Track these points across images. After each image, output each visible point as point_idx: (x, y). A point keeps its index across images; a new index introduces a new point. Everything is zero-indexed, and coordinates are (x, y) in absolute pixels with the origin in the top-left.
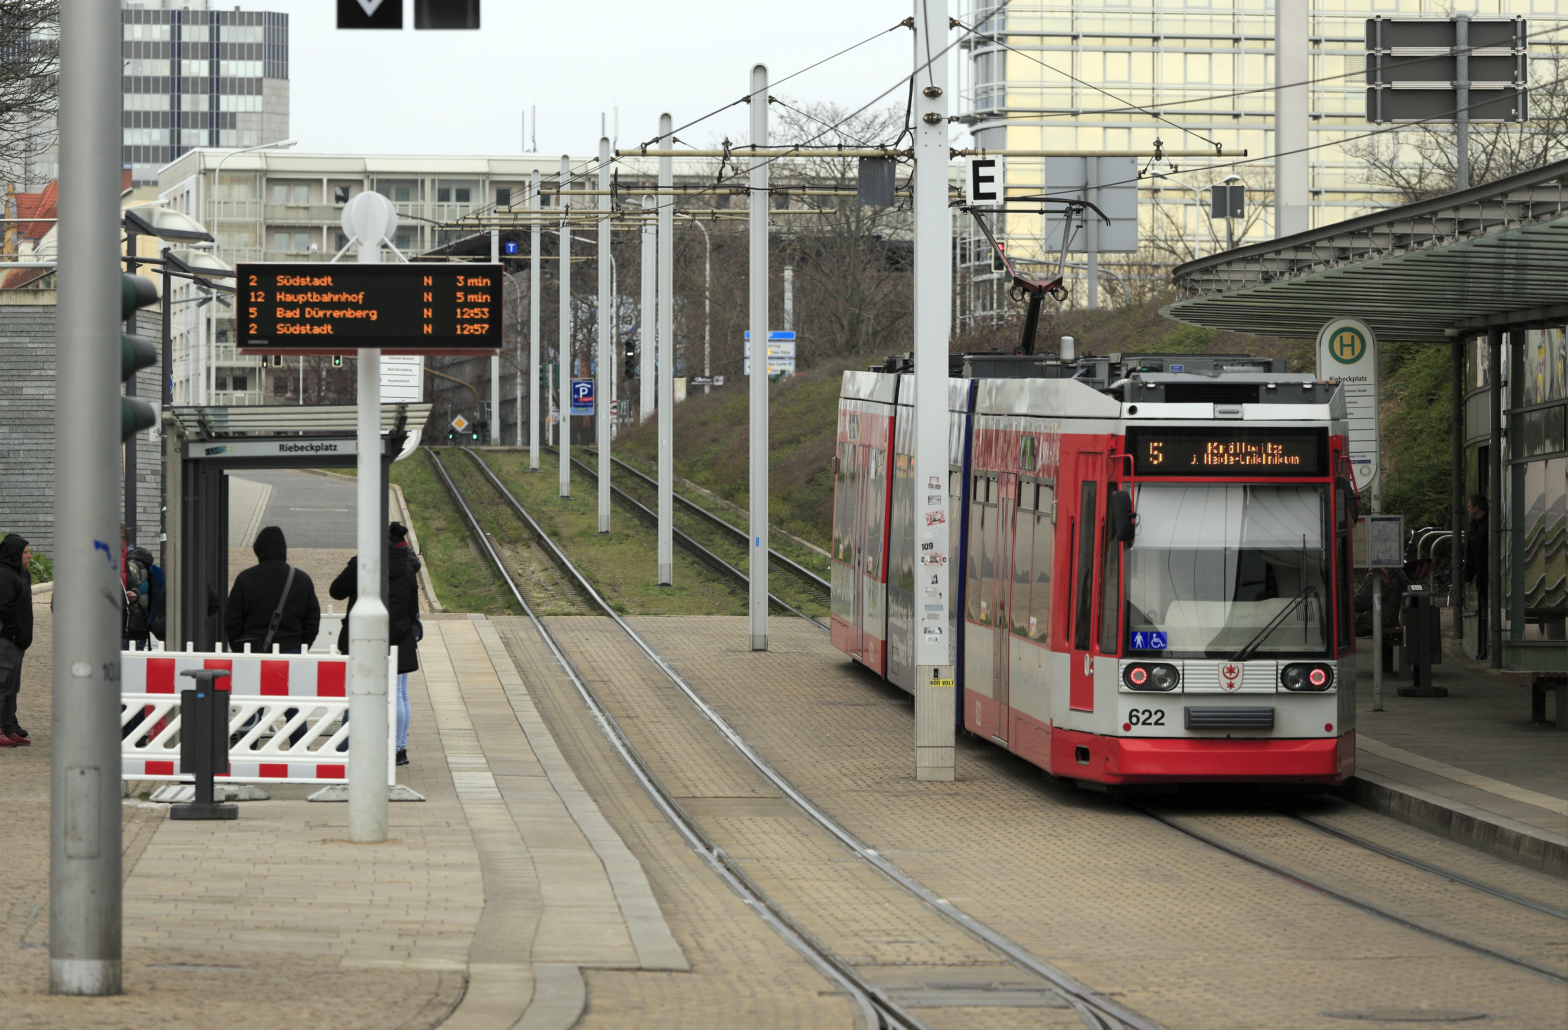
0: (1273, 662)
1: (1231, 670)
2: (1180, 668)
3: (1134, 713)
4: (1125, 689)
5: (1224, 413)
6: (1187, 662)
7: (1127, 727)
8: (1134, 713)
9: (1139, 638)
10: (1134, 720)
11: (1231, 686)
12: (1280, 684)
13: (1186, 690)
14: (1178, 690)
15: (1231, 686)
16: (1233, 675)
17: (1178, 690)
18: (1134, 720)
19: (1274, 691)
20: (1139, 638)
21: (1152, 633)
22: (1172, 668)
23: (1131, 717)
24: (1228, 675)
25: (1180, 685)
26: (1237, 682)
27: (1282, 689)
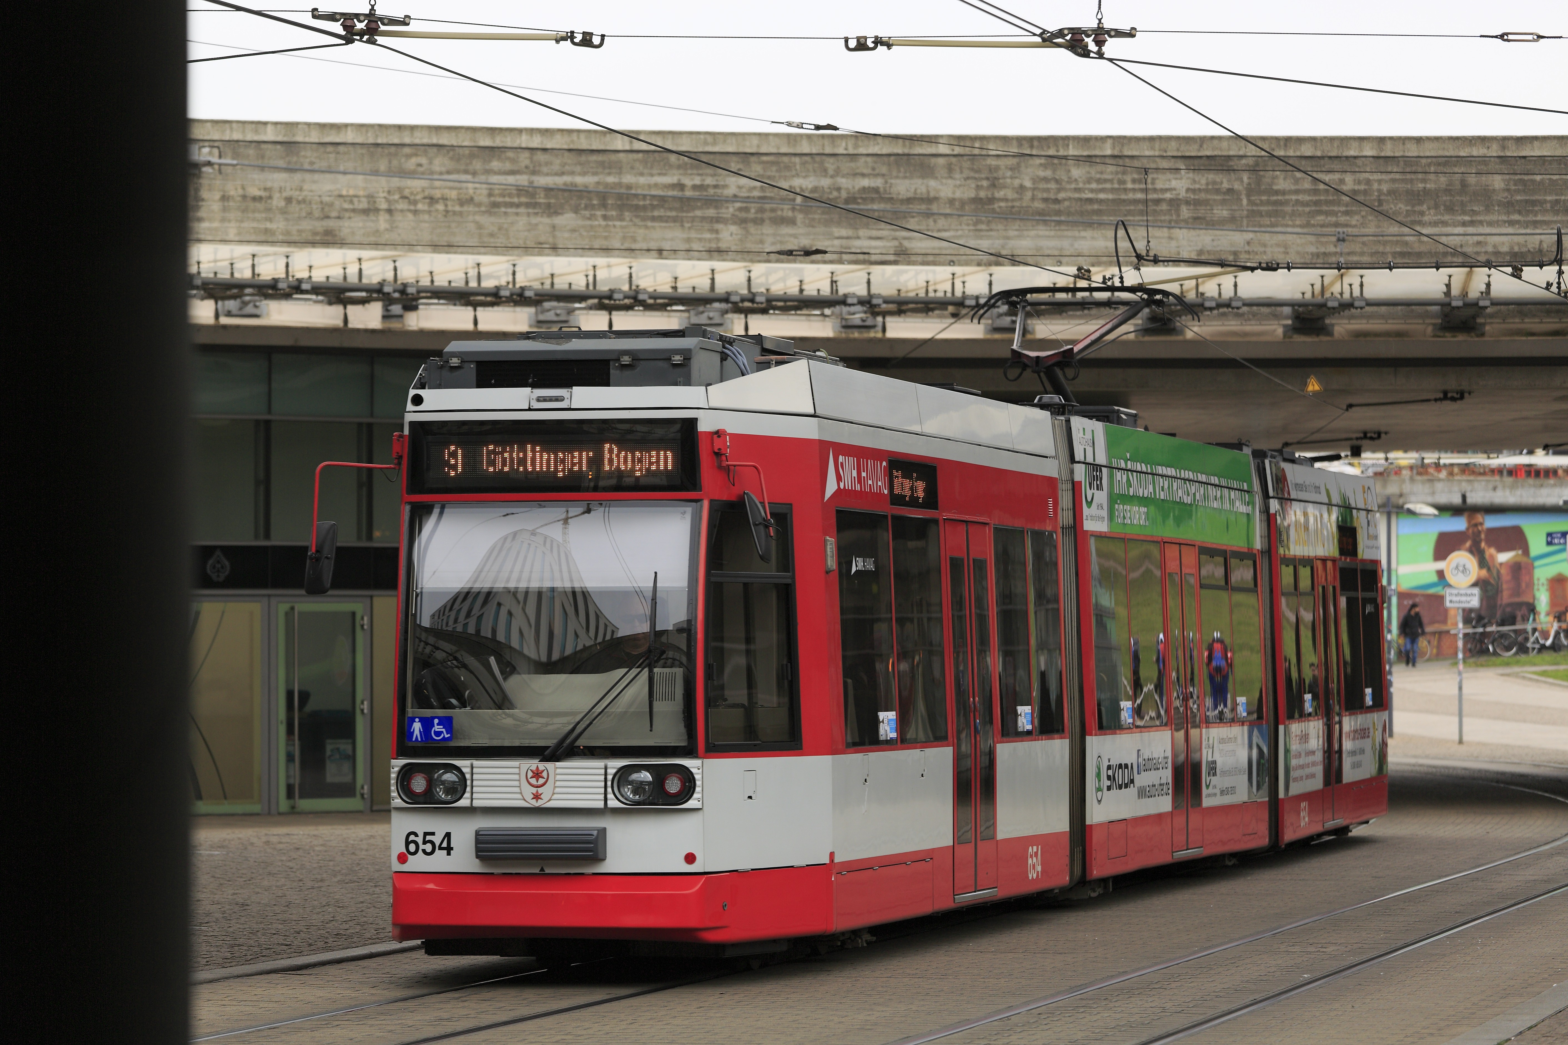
1: (537, 774)
3: (412, 838)
7: (402, 859)
8: (412, 838)
9: (417, 726)
10: (412, 847)
11: (537, 797)
12: (610, 796)
15: (537, 797)
16: (541, 781)
18: (412, 847)
19: (601, 804)
20: (417, 726)
24: (533, 781)
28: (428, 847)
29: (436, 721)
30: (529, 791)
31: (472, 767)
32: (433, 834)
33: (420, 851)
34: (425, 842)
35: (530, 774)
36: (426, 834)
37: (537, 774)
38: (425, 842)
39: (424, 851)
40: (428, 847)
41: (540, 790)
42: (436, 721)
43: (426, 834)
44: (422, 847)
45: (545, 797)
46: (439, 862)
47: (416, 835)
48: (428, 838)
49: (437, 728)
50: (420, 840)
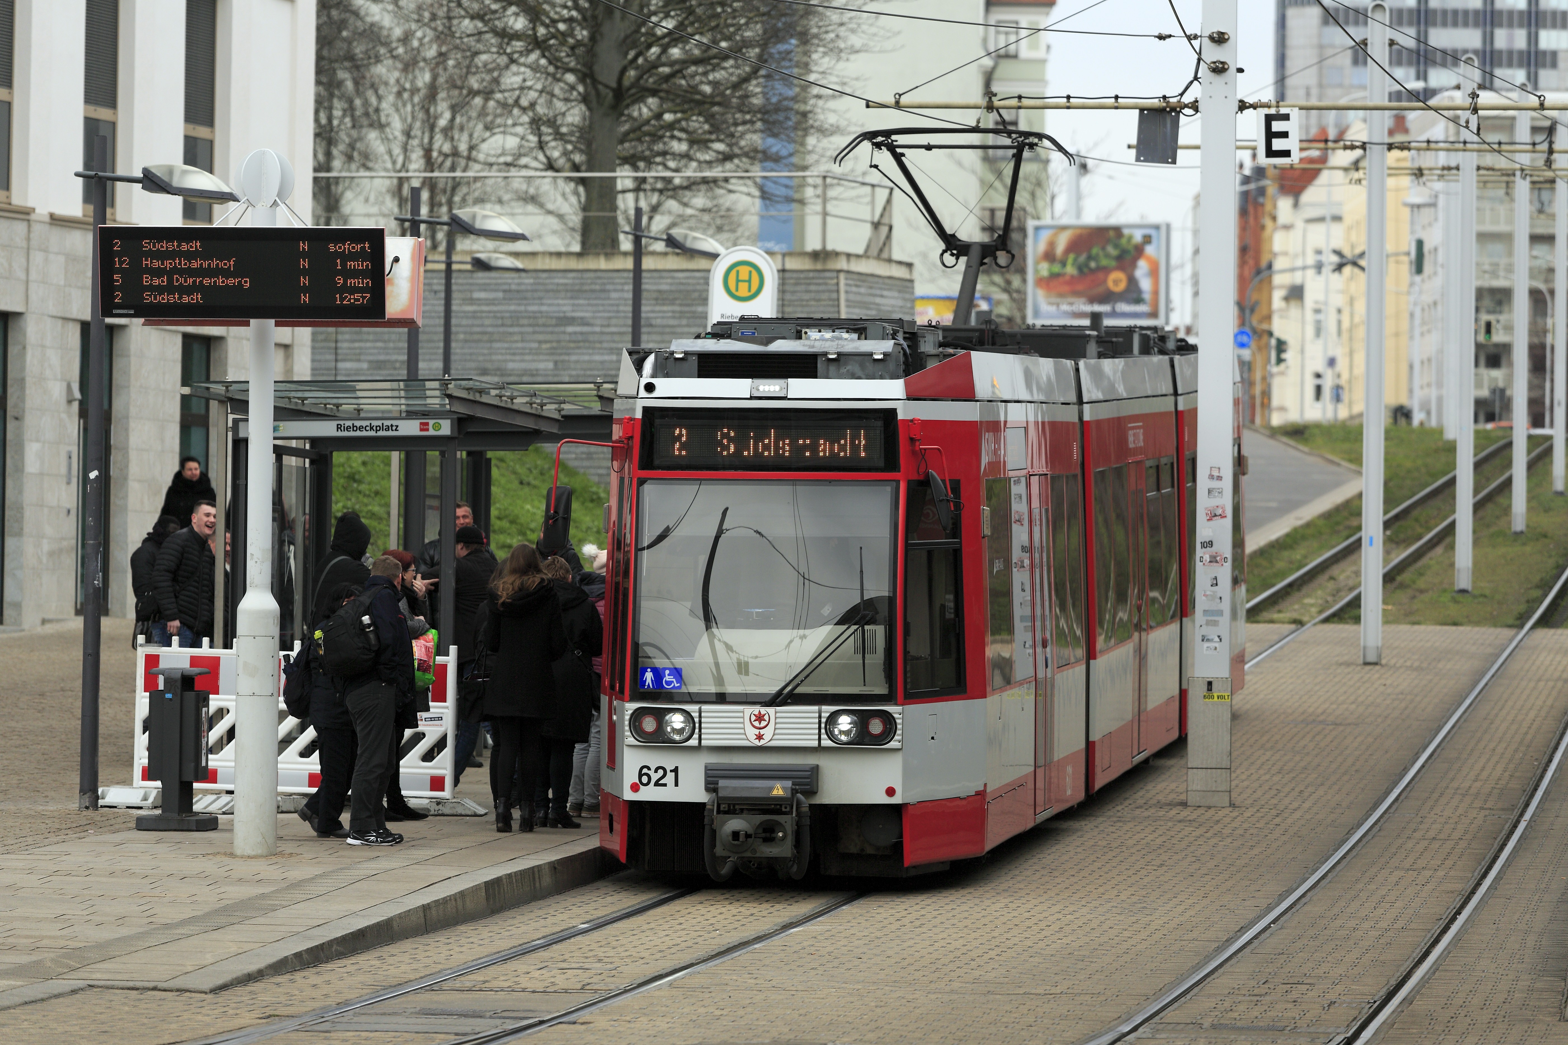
1: (760, 718)
3: (645, 771)
7: (635, 788)
8: (645, 771)
9: (649, 676)
10: (645, 779)
11: (760, 737)
15: (760, 737)
16: (763, 724)
18: (645, 779)
23: (640, 775)
24: (756, 724)
29: (667, 672)
30: (752, 733)
31: (700, 712)
35: (753, 718)
37: (760, 718)
41: (762, 731)
45: (767, 738)
47: (649, 769)
49: (667, 678)
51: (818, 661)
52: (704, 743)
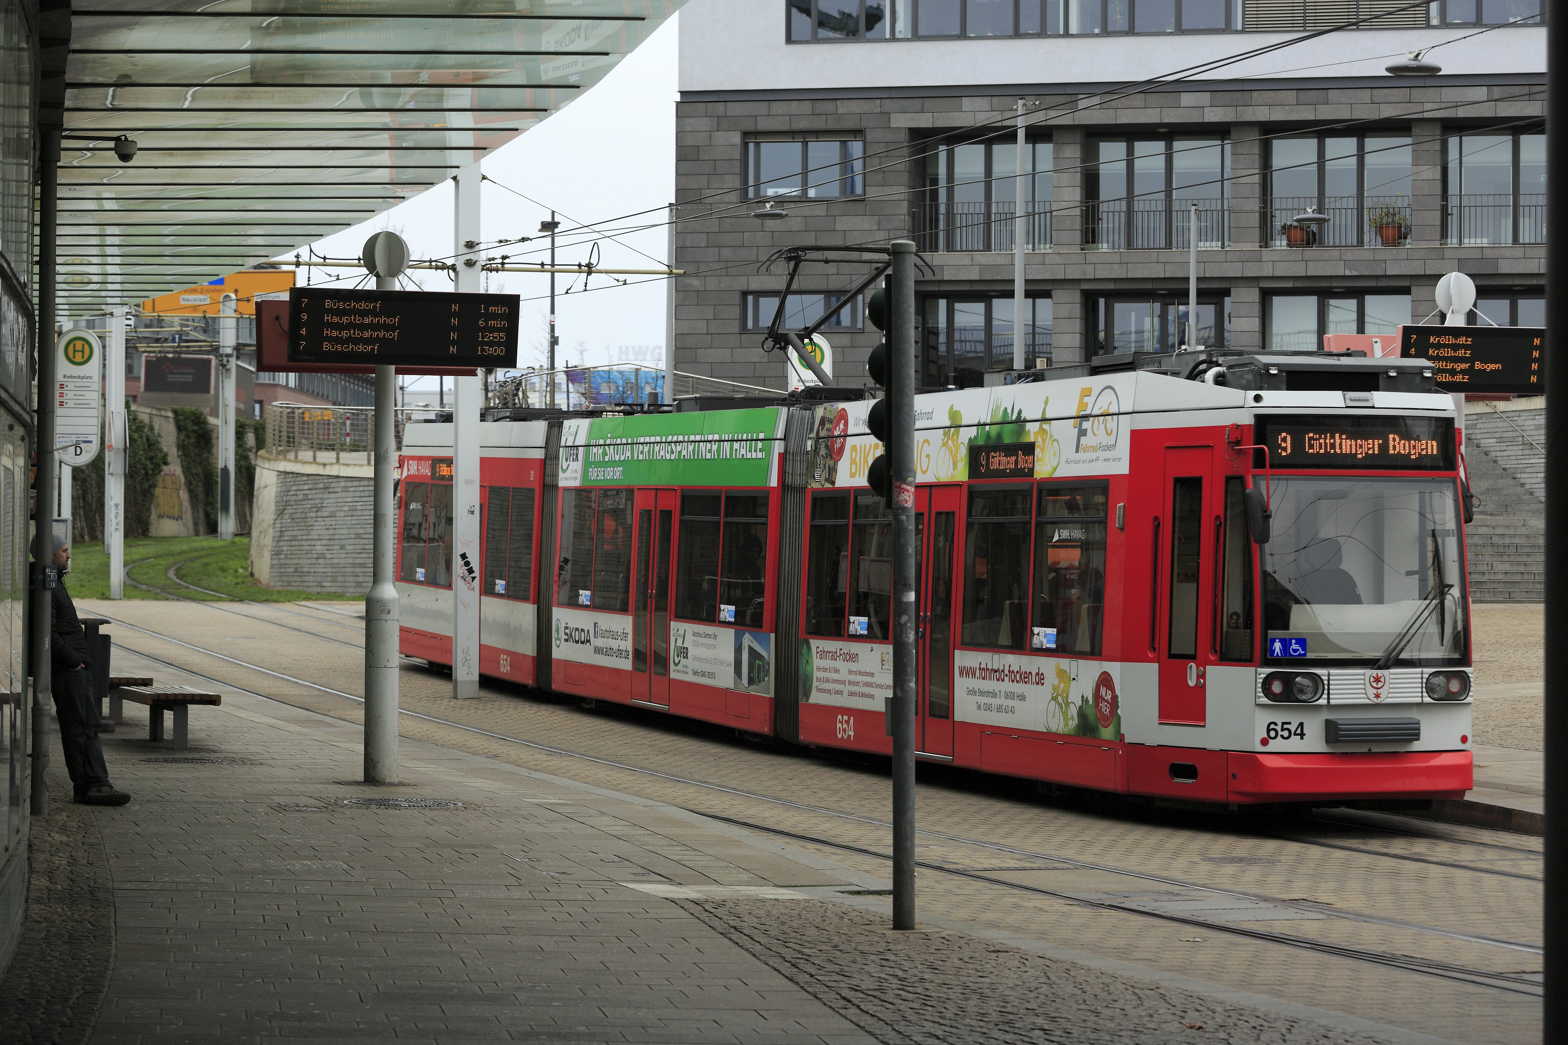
0: (1419, 670)
1: (1377, 680)
2: (1325, 678)
3: (1272, 726)
4: (1265, 700)
5: (1355, 400)
6: (1333, 671)
7: (1264, 742)
8: (1272, 726)
9: (1277, 646)
10: (1272, 734)
11: (1377, 696)
13: (1332, 702)
14: (1323, 701)
15: (1377, 696)
16: (1380, 684)
17: (1323, 701)
18: (1272, 734)
20: (1277, 646)
21: (1291, 640)
22: (1316, 678)
23: (1269, 730)
24: (1374, 684)
25: (1325, 696)
26: (1383, 692)
27: (1427, 700)
28: (1286, 734)
29: (1294, 641)
32: (1289, 723)
33: (1279, 737)
34: (1283, 730)
35: (1372, 679)
36: (1283, 723)
38: (1283, 730)
39: (1282, 736)
40: (1286, 734)
41: (1379, 691)
42: (1294, 641)
43: (1283, 723)
44: (1280, 733)
46: (1294, 745)
47: (1276, 724)
48: (1285, 726)
49: (1294, 646)
50: (1279, 728)
51: (1413, 631)
52: (1332, 702)
